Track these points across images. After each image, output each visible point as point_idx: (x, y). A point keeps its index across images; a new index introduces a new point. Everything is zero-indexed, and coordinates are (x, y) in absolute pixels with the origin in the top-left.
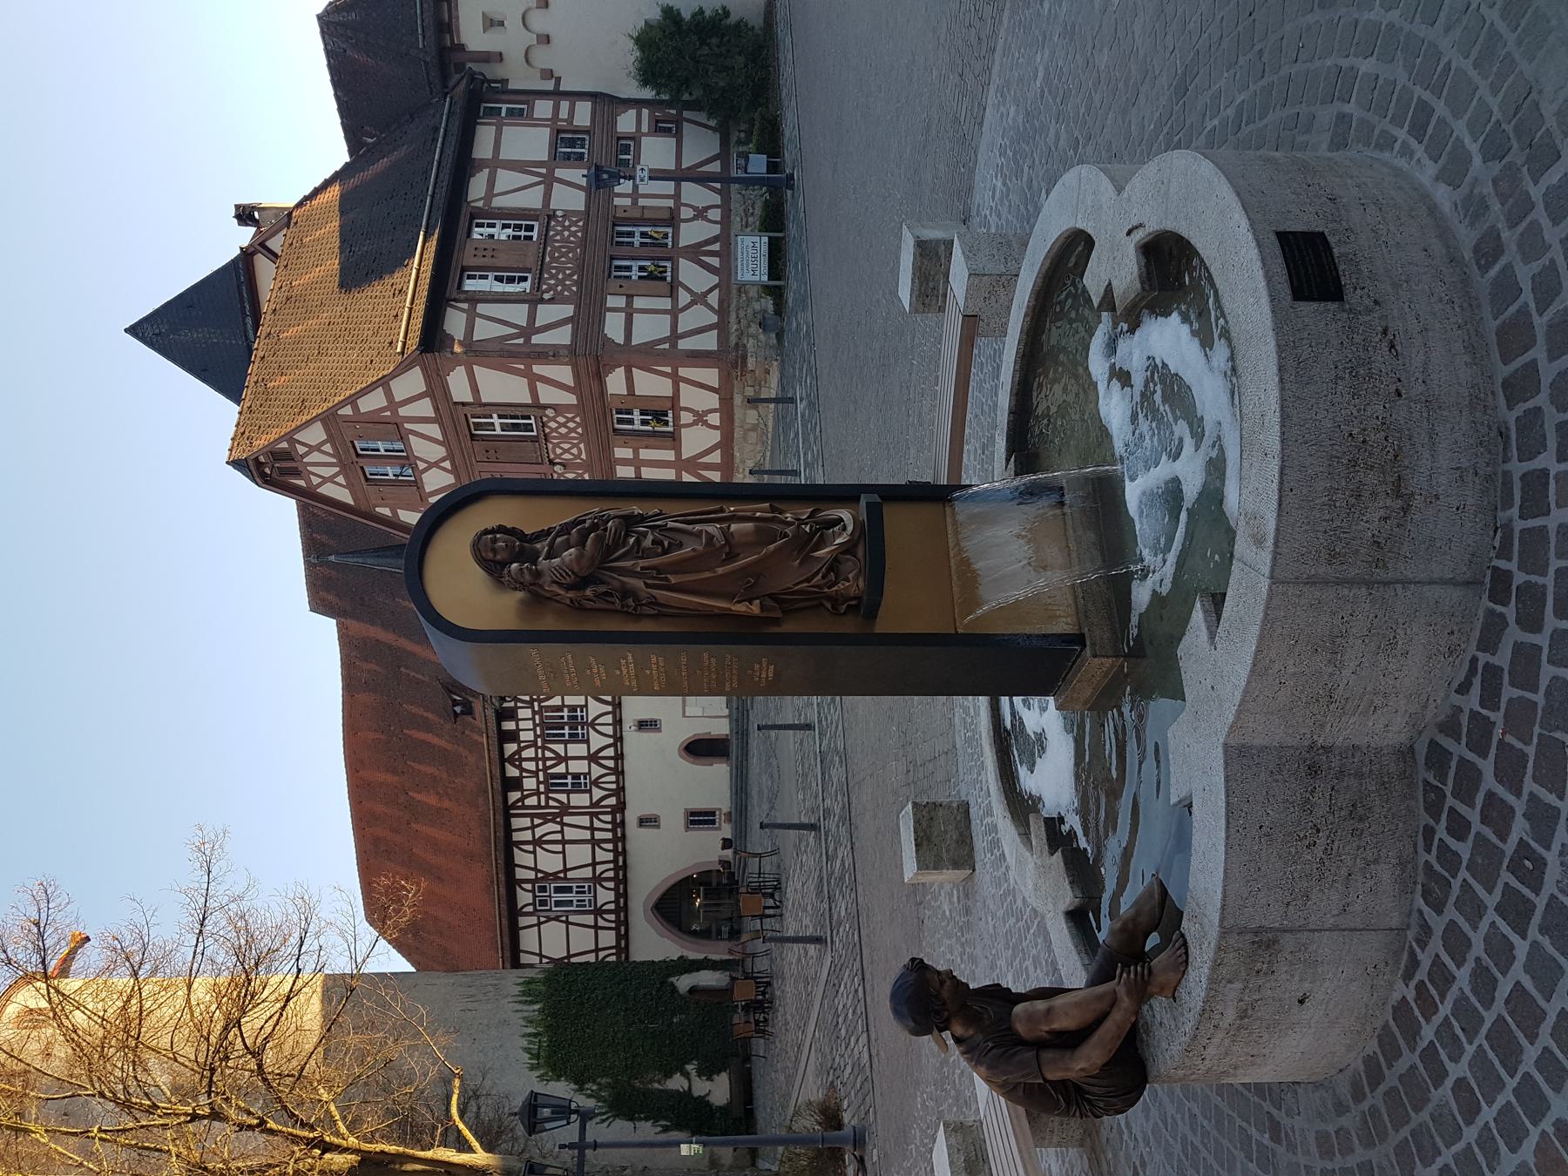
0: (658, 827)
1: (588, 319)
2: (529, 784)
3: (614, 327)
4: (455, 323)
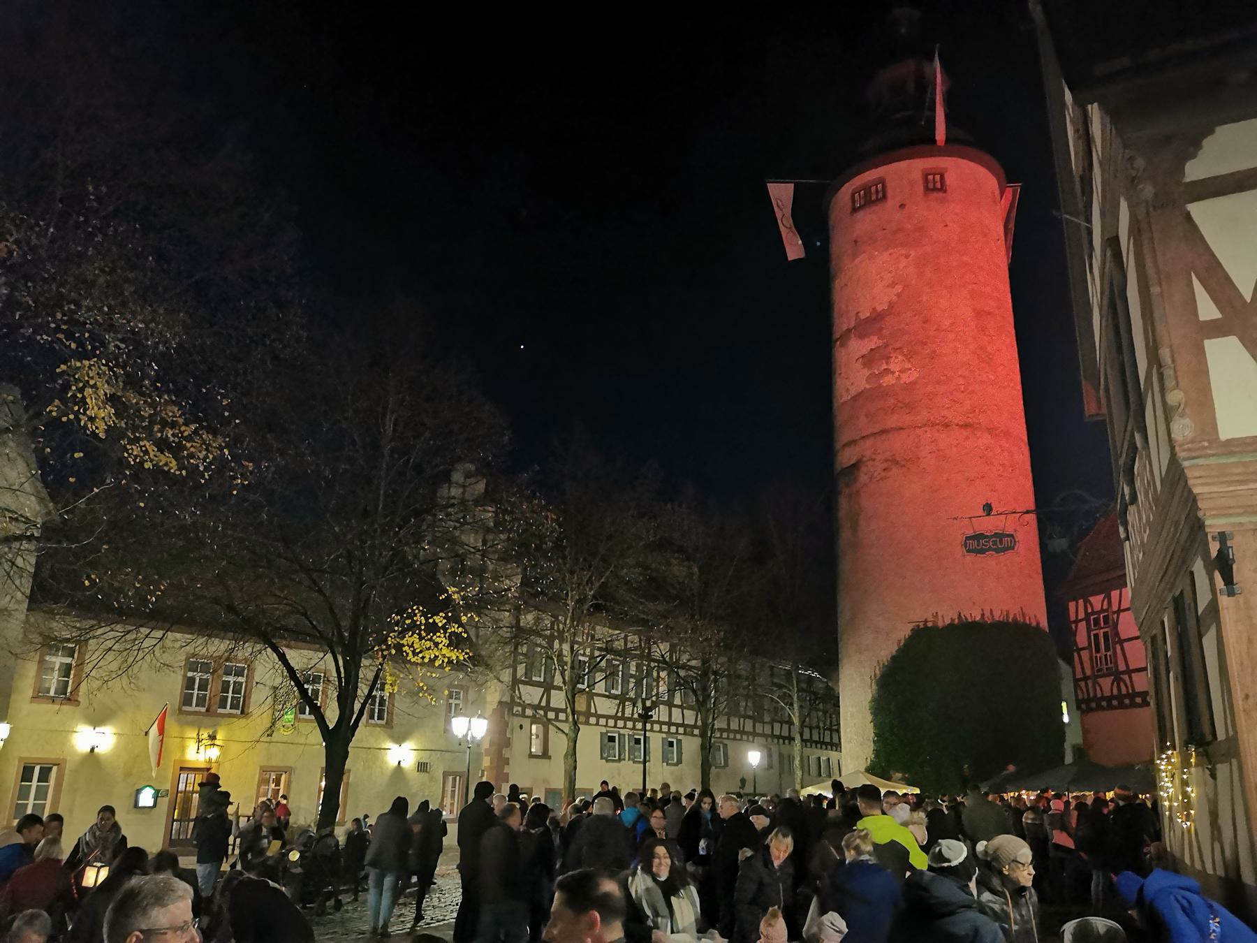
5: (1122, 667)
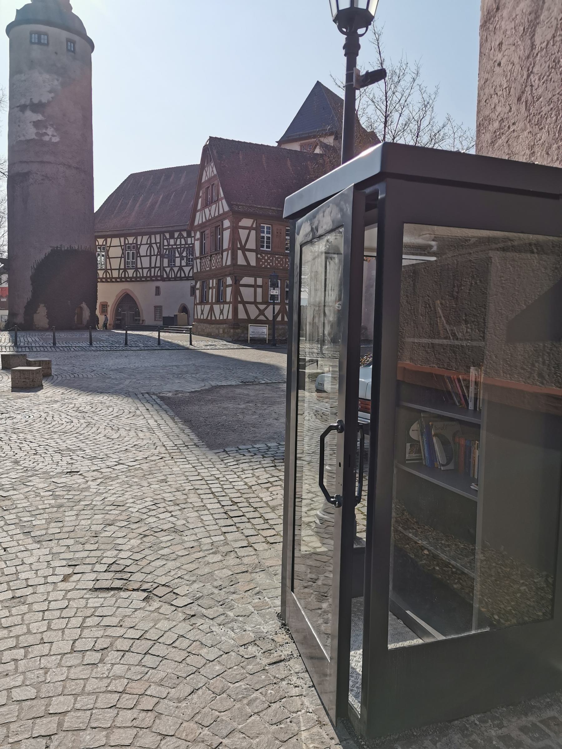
0: (156, 295)
1: (248, 270)
2: (172, 242)
3: (247, 280)
4: (246, 222)
5: (109, 267)
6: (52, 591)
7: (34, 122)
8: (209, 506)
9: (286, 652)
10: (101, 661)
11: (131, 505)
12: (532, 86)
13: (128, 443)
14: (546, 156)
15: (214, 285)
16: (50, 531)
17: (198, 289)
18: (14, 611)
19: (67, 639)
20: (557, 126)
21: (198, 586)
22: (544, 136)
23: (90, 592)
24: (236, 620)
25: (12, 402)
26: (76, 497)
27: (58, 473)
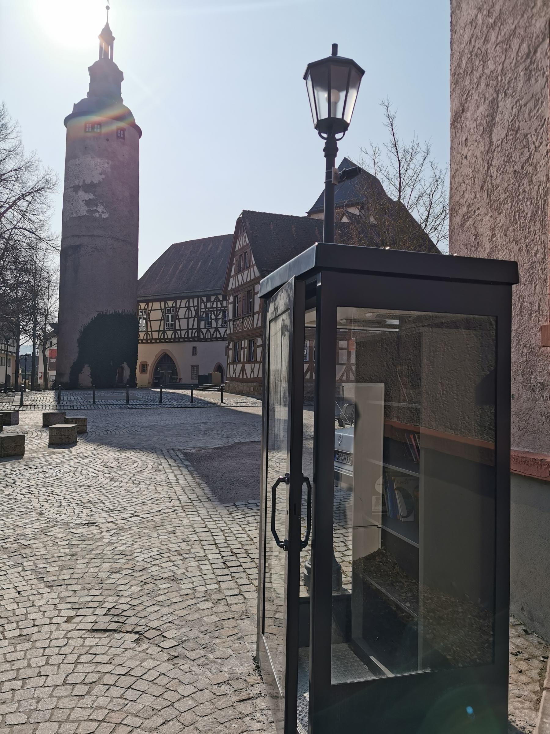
0: (193, 355)
2: (209, 305)
5: (149, 329)
6: (55, 631)
7: (86, 201)
8: (210, 556)
9: (256, 690)
10: (88, 693)
11: (138, 555)
12: (491, 176)
13: (146, 496)
14: (504, 237)
15: (246, 346)
16: (61, 577)
17: (231, 349)
18: (19, 647)
19: (61, 672)
20: (512, 211)
21: (185, 631)
22: (502, 220)
23: (89, 633)
24: (215, 662)
25: (47, 458)
26: (89, 547)
27: (77, 524)
